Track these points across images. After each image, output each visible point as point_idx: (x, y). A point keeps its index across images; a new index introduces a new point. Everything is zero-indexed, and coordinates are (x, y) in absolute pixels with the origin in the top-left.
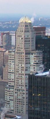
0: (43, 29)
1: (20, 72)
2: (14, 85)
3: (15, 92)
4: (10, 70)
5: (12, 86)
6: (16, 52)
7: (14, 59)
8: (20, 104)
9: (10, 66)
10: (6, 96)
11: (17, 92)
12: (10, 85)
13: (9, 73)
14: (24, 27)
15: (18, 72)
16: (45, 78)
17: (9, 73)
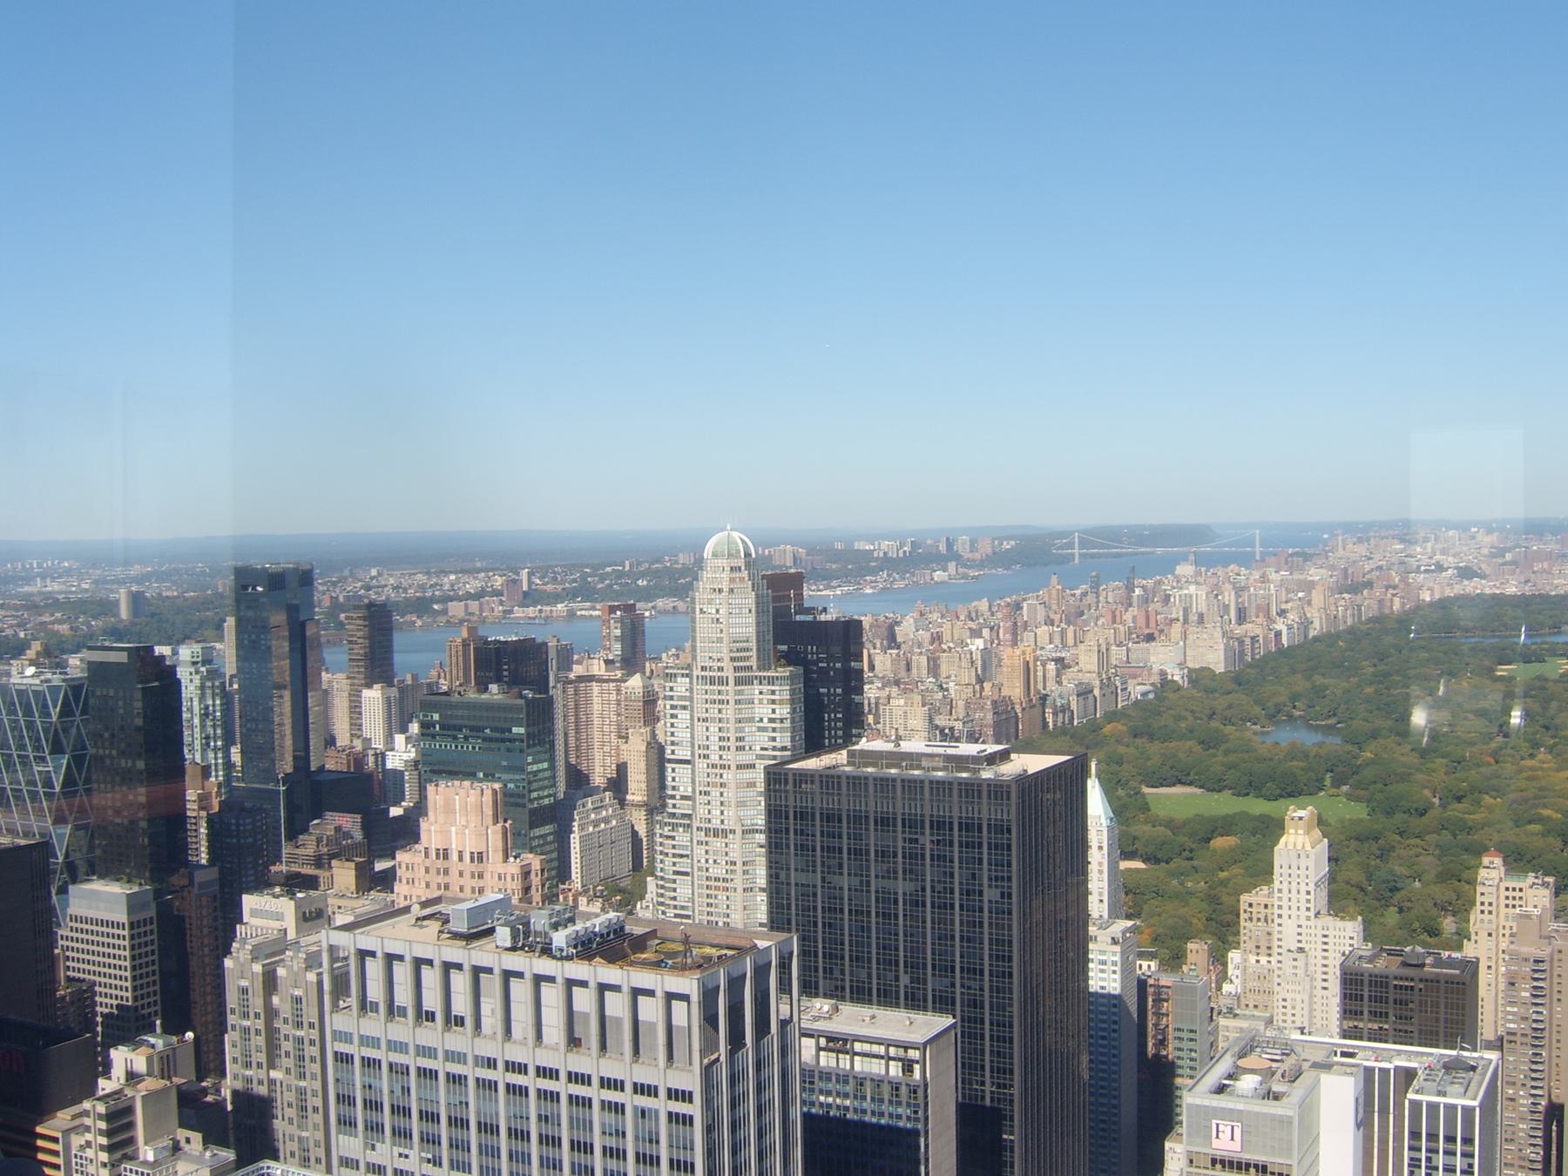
0: (796, 581)
1: (714, 758)
2: (690, 812)
3: (695, 842)
4: (673, 752)
5: (684, 816)
6: (698, 677)
7: (688, 703)
8: (717, 888)
9: (673, 734)
10: (659, 857)
11: (704, 839)
12: (674, 814)
13: (670, 761)
14: (726, 575)
15: (706, 757)
16: (833, 777)
17: (670, 761)
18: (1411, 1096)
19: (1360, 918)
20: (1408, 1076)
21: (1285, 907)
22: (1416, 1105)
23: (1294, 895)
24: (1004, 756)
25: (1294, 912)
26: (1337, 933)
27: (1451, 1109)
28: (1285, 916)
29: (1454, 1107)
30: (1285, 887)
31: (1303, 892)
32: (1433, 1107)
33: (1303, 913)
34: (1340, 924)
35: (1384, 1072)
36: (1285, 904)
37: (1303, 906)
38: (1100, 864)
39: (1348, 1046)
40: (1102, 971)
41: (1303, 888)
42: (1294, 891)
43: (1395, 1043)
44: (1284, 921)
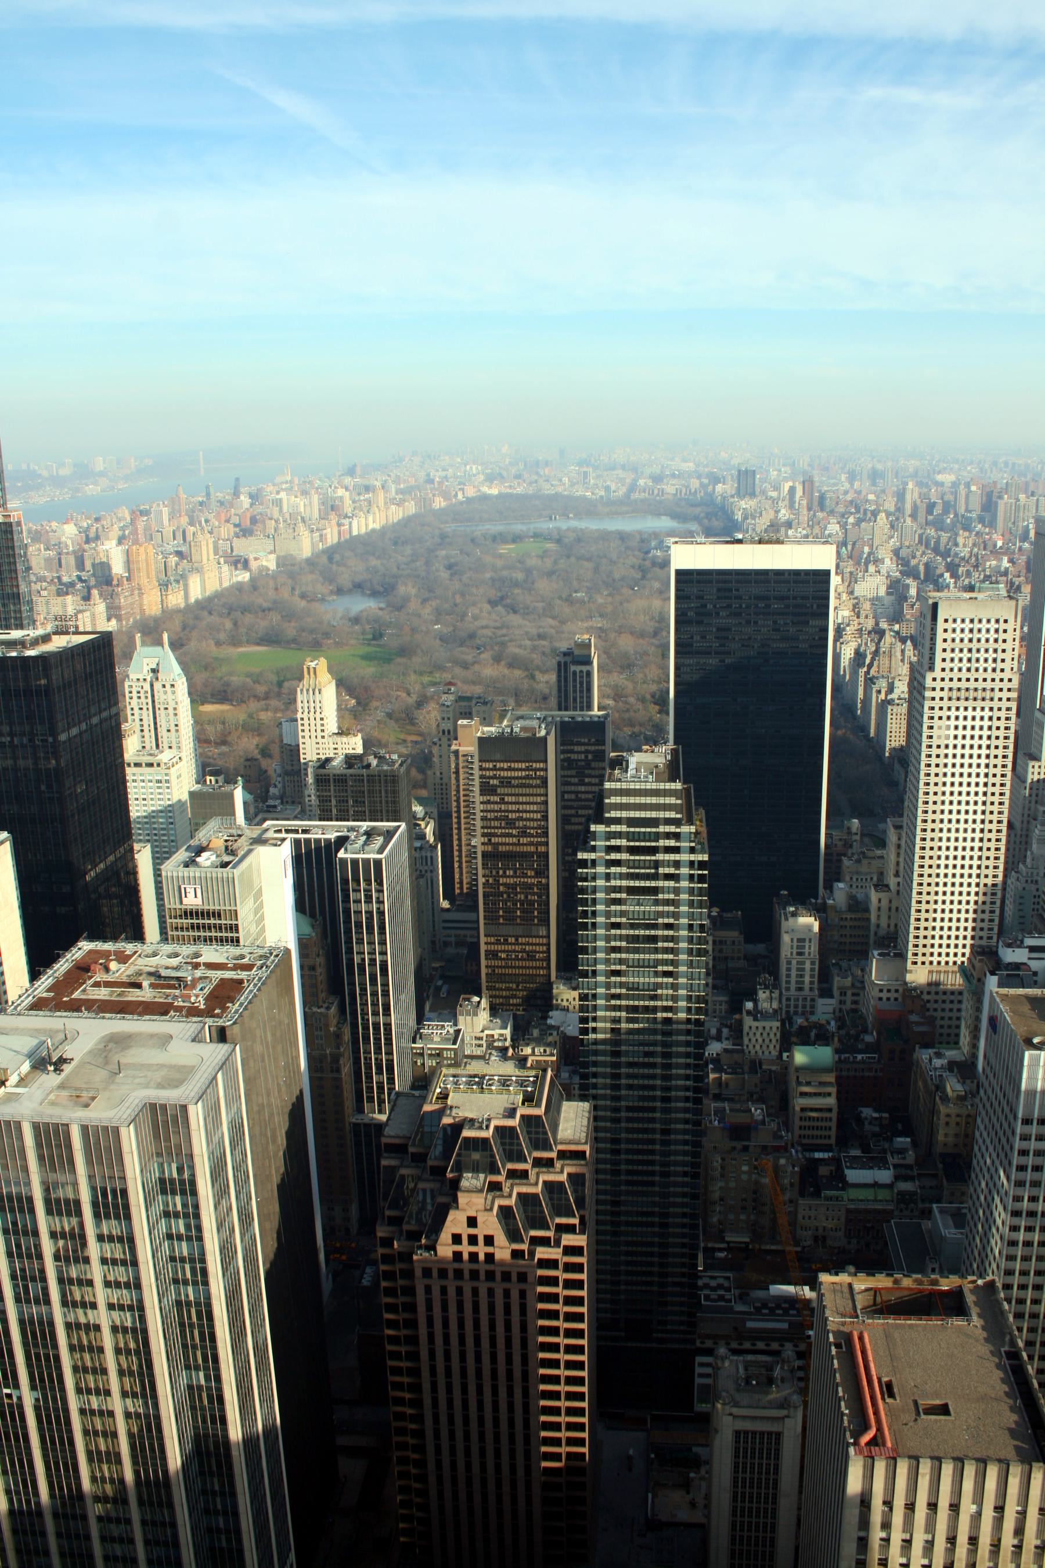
18: (341, 854)
19: (360, 735)
20: (342, 841)
21: (307, 731)
22: (344, 861)
23: (313, 722)
24: (46, 639)
25: (313, 734)
26: (344, 746)
27: (367, 862)
28: (307, 737)
29: (368, 860)
30: (305, 716)
31: (318, 719)
32: (355, 862)
33: (320, 734)
34: (345, 739)
35: (328, 842)
36: (306, 728)
37: (319, 728)
38: (175, 709)
39: (306, 826)
40: (159, 788)
41: (318, 716)
42: (312, 719)
43: (354, 820)
44: (307, 740)
